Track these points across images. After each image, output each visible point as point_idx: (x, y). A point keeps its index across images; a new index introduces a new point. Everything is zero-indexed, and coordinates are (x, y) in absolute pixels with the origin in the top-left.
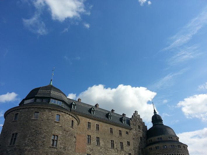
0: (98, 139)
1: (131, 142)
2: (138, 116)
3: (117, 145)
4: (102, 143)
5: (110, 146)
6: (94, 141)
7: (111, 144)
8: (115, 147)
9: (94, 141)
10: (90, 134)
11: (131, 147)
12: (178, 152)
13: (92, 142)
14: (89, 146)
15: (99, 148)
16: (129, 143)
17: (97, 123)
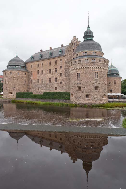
0: (42, 70)
1: (64, 66)
2: (75, 40)
3: (53, 71)
4: (44, 72)
5: (48, 72)
6: (40, 73)
7: (49, 71)
8: (52, 72)
9: (40, 73)
10: (39, 69)
11: (63, 69)
12: (73, 68)
13: (40, 73)
14: (38, 76)
15: (43, 75)
16: (61, 67)
17: (42, 62)
